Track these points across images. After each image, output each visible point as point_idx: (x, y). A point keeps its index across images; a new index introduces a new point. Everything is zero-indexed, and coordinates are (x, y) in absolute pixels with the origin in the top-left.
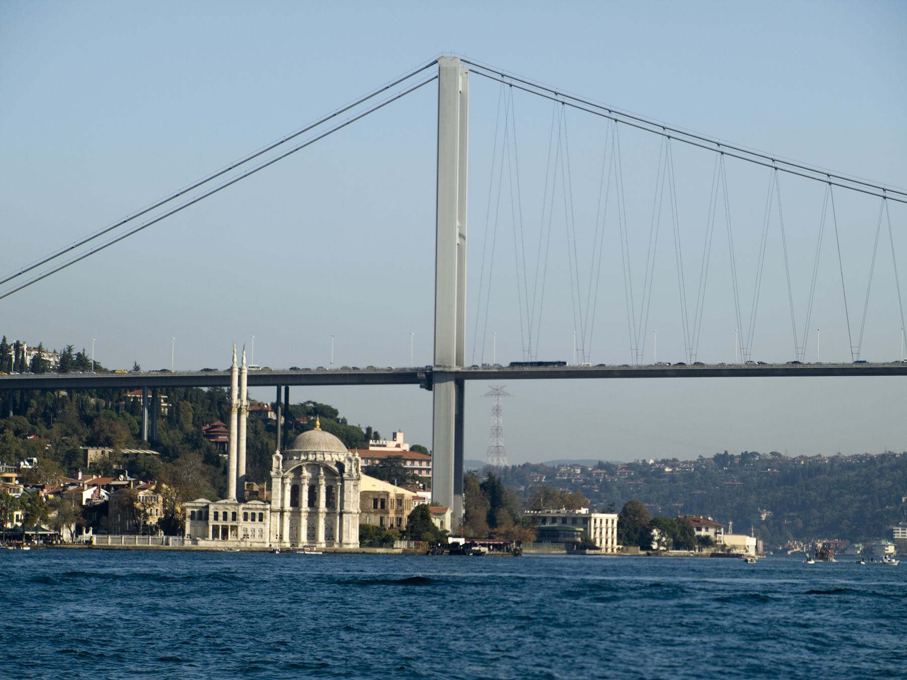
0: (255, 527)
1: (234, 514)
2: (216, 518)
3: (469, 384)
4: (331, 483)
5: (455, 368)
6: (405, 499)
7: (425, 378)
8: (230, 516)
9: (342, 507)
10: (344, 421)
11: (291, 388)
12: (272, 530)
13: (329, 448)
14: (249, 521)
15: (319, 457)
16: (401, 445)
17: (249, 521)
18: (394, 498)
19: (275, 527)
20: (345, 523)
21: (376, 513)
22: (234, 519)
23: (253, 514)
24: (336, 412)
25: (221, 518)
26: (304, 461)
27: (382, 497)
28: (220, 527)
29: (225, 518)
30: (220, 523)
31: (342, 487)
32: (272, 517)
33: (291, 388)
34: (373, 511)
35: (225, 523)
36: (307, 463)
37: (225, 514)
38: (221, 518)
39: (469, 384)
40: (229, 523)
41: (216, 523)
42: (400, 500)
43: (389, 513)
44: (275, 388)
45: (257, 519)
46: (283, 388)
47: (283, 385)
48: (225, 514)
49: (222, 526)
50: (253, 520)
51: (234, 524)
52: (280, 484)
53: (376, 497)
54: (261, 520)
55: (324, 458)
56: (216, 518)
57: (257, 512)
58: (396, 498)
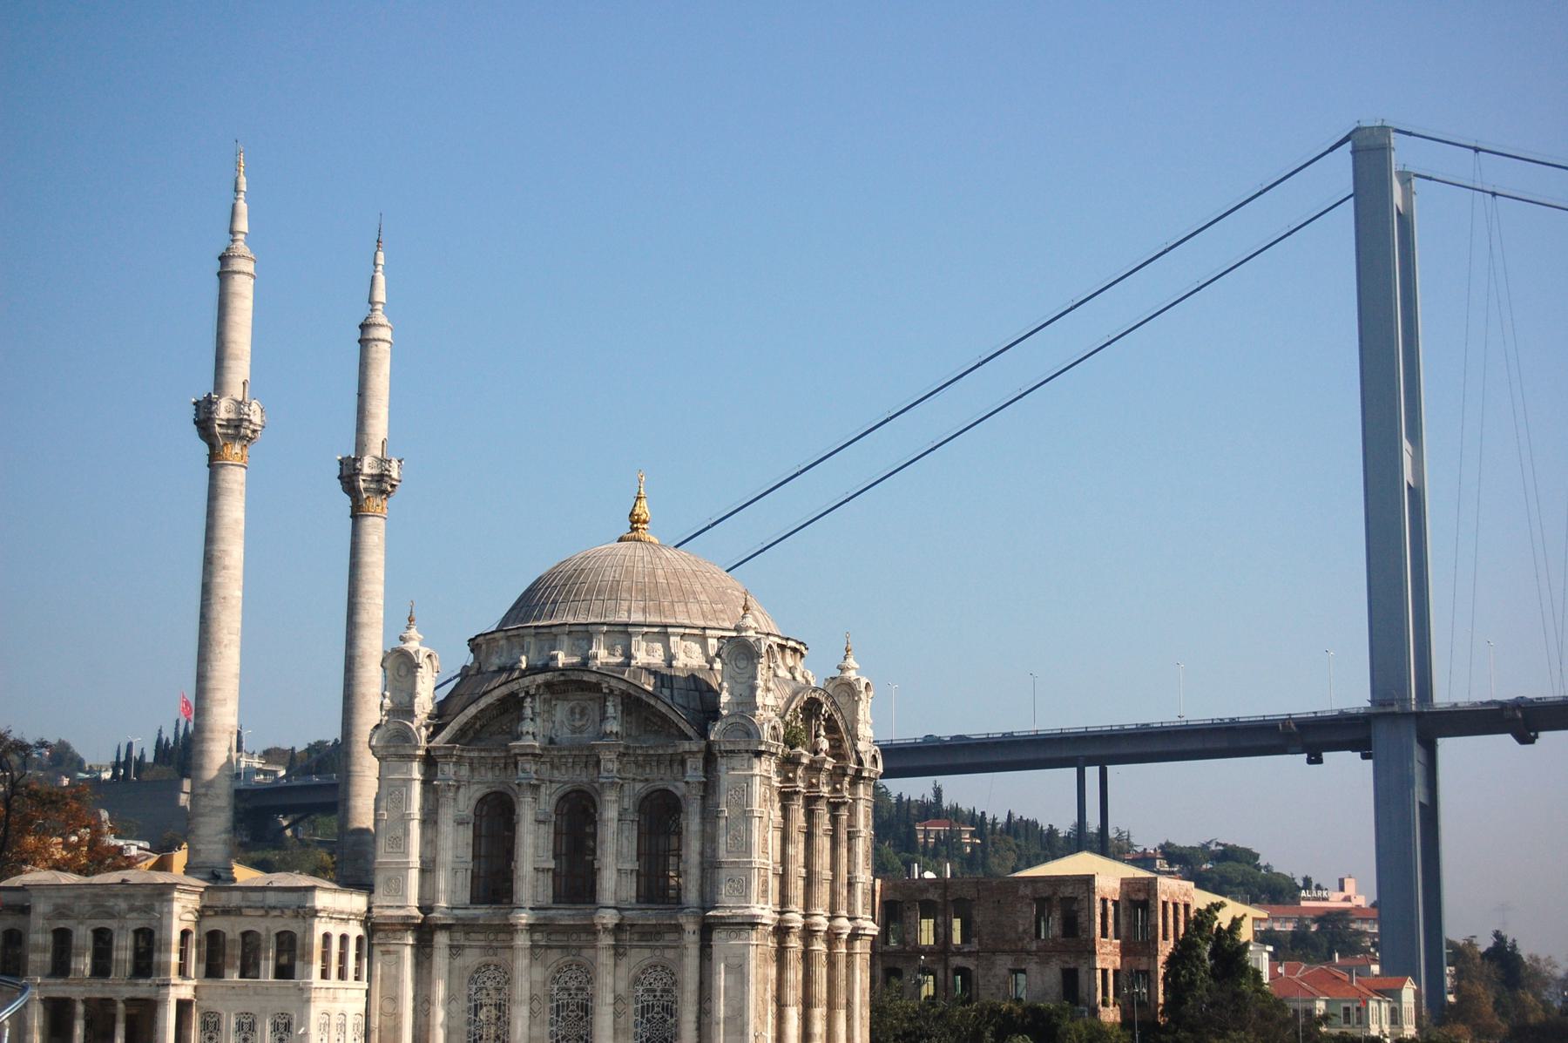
0: (253, 1005)
3: (1448, 747)
4: (662, 778)
6: (1162, 897)
8: (123, 950)
9: (708, 900)
11: (1110, 768)
12: (375, 1022)
13: (660, 611)
14: (233, 976)
15: (602, 655)
16: (1352, 898)
17: (233, 976)
19: (389, 1008)
24: (1256, 857)
25: (84, 964)
26: (532, 670)
27: (1068, 891)
28: (80, 1009)
29: (101, 968)
30: (81, 985)
31: (709, 787)
32: (377, 951)
33: (1110, 768)
35: (98, 990)
36: (540, 678)
37: (103, 940)
39: (1448, 747)
40: (121, 988)
41: (58, 989)
43: (1093, 953)
44: (1073, 771)
45: (268, 966)
46: (1092, 773)
47: (1091, 762)
48: (103, 940)
49: (86, 1002)
50: (249, 968)
51: (143, 989)
52: (417, 789)
54: (284, 972)
55: (628, 656)
56: (61, 968)
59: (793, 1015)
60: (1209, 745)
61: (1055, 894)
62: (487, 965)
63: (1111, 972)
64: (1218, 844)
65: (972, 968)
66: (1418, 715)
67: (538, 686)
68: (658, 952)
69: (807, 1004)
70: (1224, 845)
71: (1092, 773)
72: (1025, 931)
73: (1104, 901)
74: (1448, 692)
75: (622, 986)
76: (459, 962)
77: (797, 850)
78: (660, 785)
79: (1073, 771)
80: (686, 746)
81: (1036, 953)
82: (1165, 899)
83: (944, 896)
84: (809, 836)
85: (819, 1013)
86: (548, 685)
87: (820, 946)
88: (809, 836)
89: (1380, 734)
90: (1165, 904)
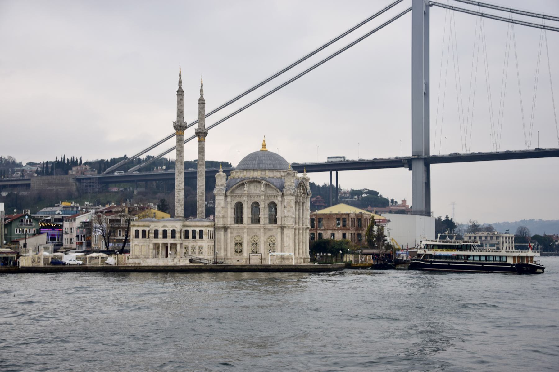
0: (195, 244)
1: (173, 232)
2: (156, 236)
3: (433, 166)
5: (424, 156)
7: (407, 162)
8: (169, 234)
10: (381, 196)
11: (339, 172)
18: (355, 218)
20: (286, 239)
21: (338, 229)
22: (173, 236)
23: (194, 232)
24: (378, 193)
25: (160, 236)
27: (344, 216)
30: (160, 241)
34: (336, 228)
35: (165, 241)
37: (165, 232)
38: (160, 236)
39: (433, 166)
40: (169, 241)
41: (156, 241)
42: (359, 218)
44: (329, 173)
45: (197, 236)
46: (334, 173)
47: (334, 170)
48: (165, 232)
53: (339, 217)
54: (201, 237)
56: (156, 236)
57: (197, 230)
58: (357, 217)
59: (297, 245)
60: (367, 166)
61: (341, 217)
62: (238, 236)
63: (353, 234)
64: (366, 189)
65: (323, 233)
66: (425, 159)
67: (248, 182)
68: (272, 233)
69: (299, 243)
70: (369, 190)
71: (334, 173)
72: (334, 225)
73: (352, 218)
74: (434, 151)
75: (265, 240)
76: (232, 235)
77: (297, 213)
78: (272, 201)
79: (329, 173)
80: (278, 194)
81: (337, 230)
82: (365, 218)
83: (316, 217)
84: (299, 209)
85: (301, 244)
86: (248, 182)
87: (301, 231)
88: (299, 209)
89: (414, 164)
90: (365, 219)
